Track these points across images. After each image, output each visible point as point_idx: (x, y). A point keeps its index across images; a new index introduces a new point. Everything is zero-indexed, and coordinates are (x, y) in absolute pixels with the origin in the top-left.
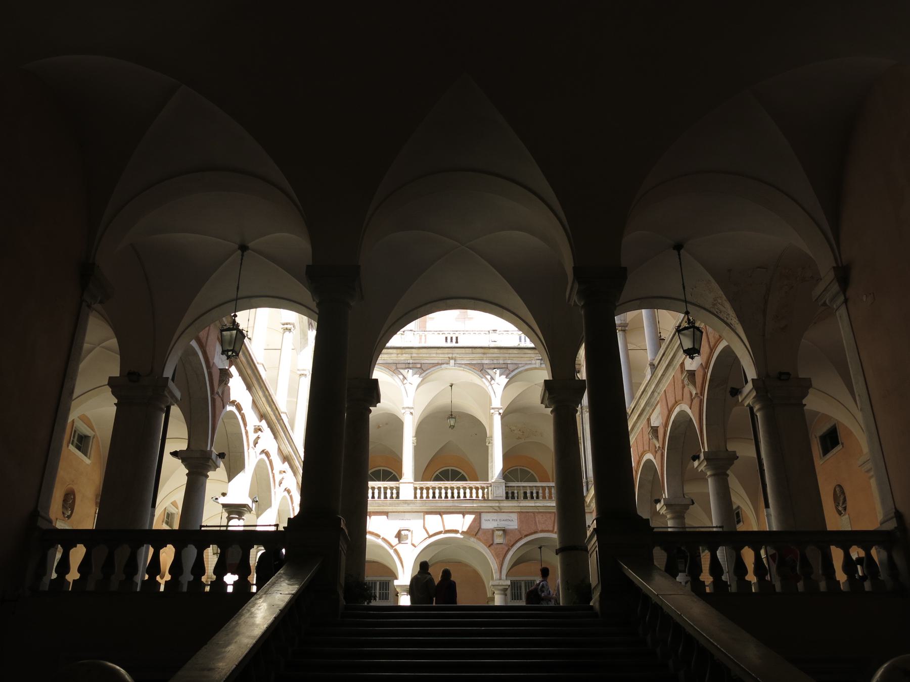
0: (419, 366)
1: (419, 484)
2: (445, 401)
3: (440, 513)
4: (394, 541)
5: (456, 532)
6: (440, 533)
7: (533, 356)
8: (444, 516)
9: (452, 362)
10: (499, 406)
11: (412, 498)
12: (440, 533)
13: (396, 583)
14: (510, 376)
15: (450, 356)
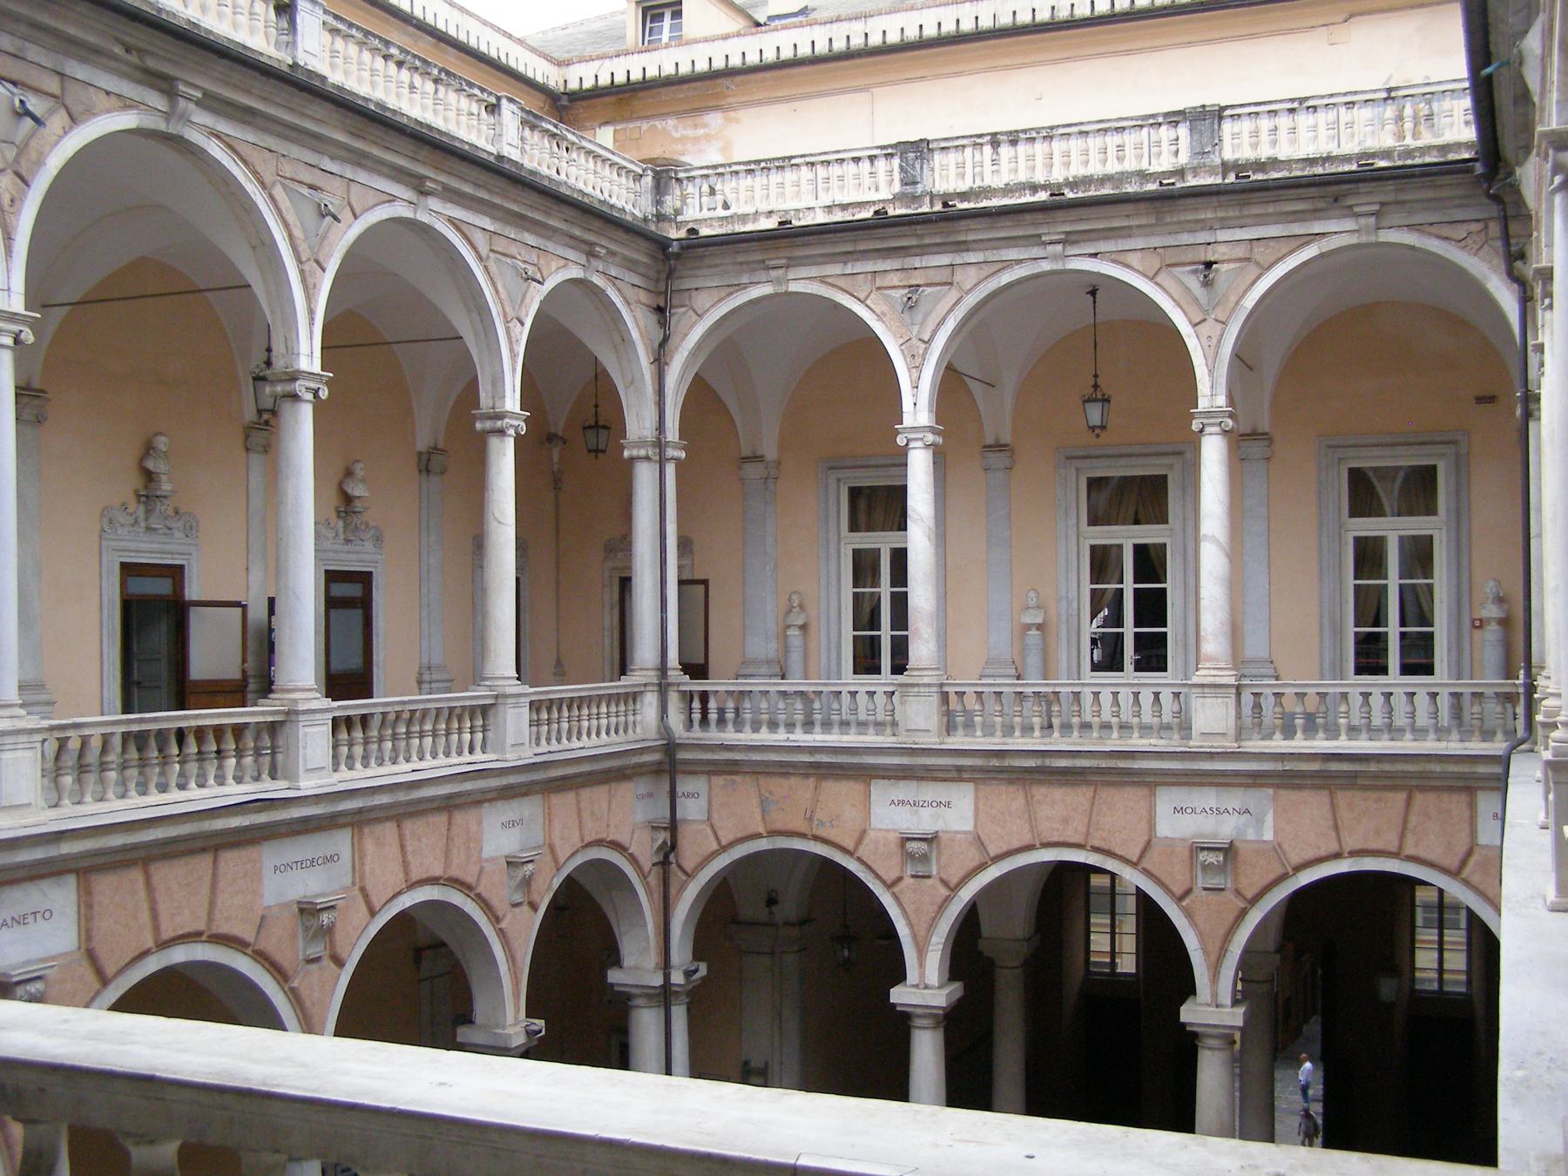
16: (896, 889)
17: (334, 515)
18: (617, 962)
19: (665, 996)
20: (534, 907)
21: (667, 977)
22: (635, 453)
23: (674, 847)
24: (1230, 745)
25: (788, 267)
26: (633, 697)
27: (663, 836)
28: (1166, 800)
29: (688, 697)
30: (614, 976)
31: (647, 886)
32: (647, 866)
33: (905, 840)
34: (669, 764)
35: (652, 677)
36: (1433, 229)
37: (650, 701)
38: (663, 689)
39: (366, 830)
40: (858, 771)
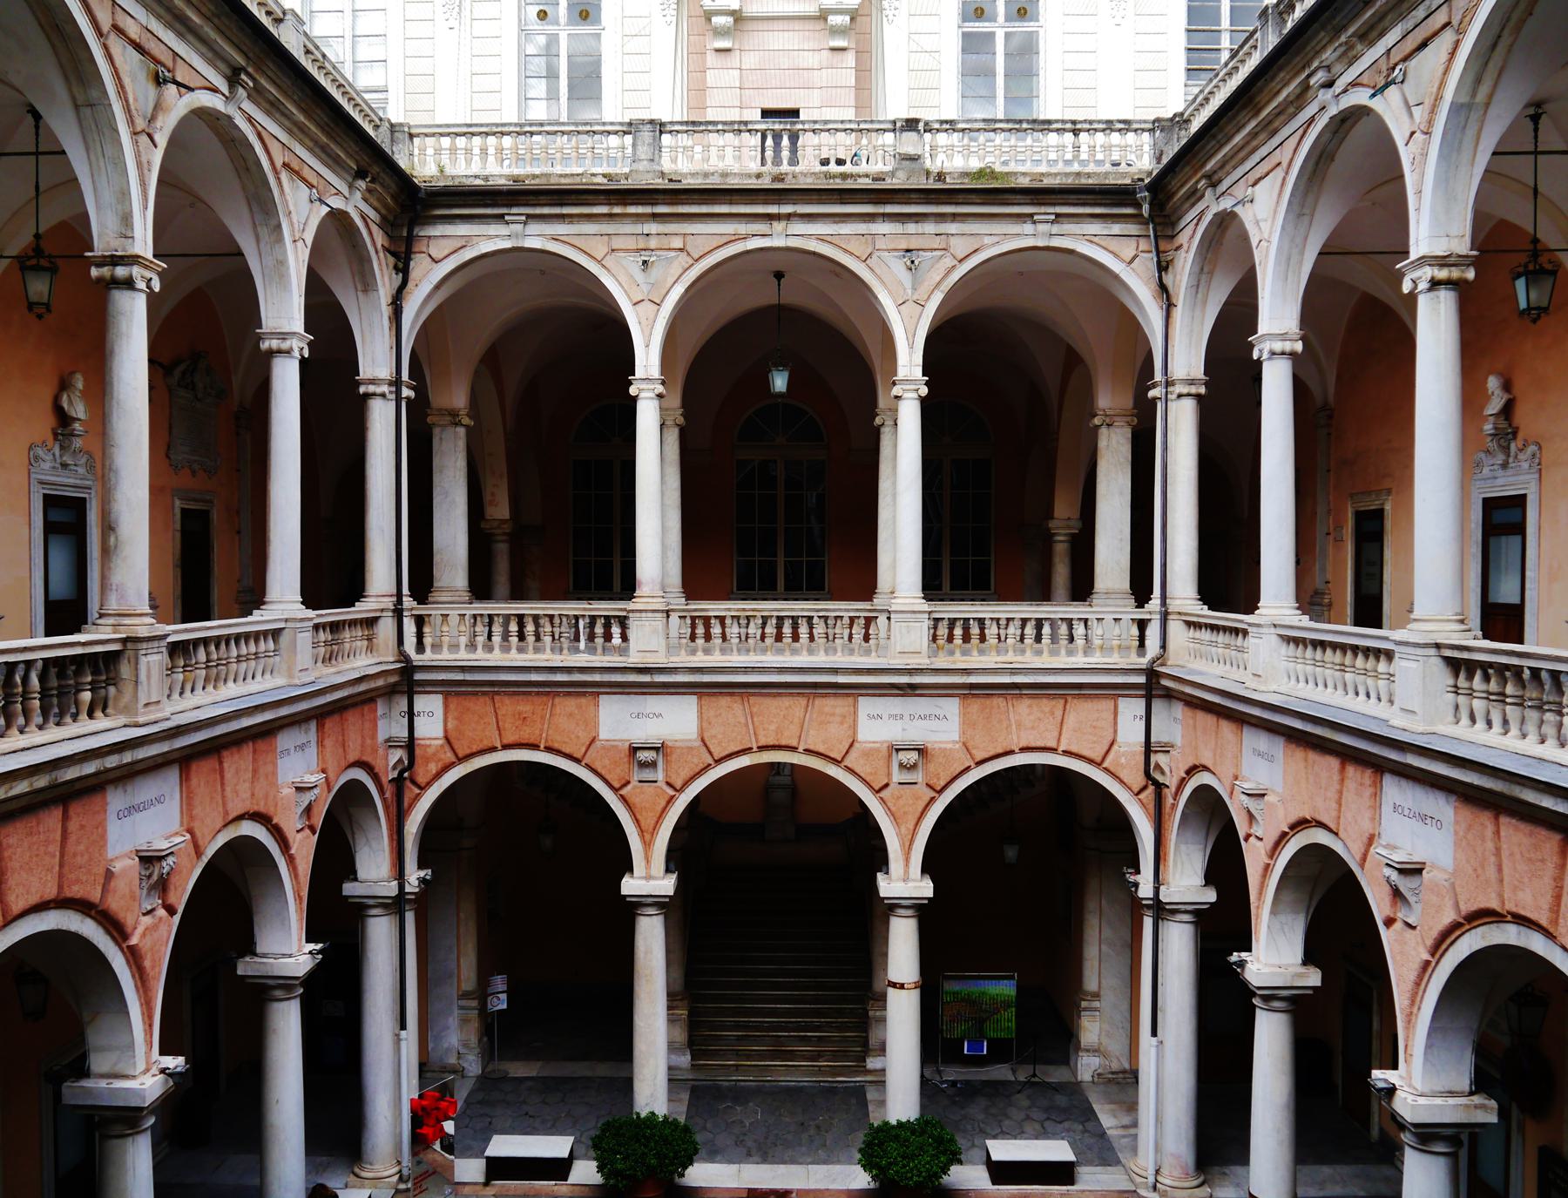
0: (677, 243)
9: (778, 226)
16: (623, 792)
17: (51, 437)
19: (396, 906)
20: (312, 829)
21: (401, 887)
22: (371, 389)
24: (923, 661)
25: (525, 223)
26: (370, 623)
27: (396, 755)
28: (867, 705)
29: (420, 621)
30: (349, 889)
31: (384, 800)
32: (384, 780)
33: (634, 750)
34: (406, 682)
35: (389, 603)
36: (1096, 239)
37: (386, 627)
38: (398, 613)
39: (194, 767)
40: (587, 688)
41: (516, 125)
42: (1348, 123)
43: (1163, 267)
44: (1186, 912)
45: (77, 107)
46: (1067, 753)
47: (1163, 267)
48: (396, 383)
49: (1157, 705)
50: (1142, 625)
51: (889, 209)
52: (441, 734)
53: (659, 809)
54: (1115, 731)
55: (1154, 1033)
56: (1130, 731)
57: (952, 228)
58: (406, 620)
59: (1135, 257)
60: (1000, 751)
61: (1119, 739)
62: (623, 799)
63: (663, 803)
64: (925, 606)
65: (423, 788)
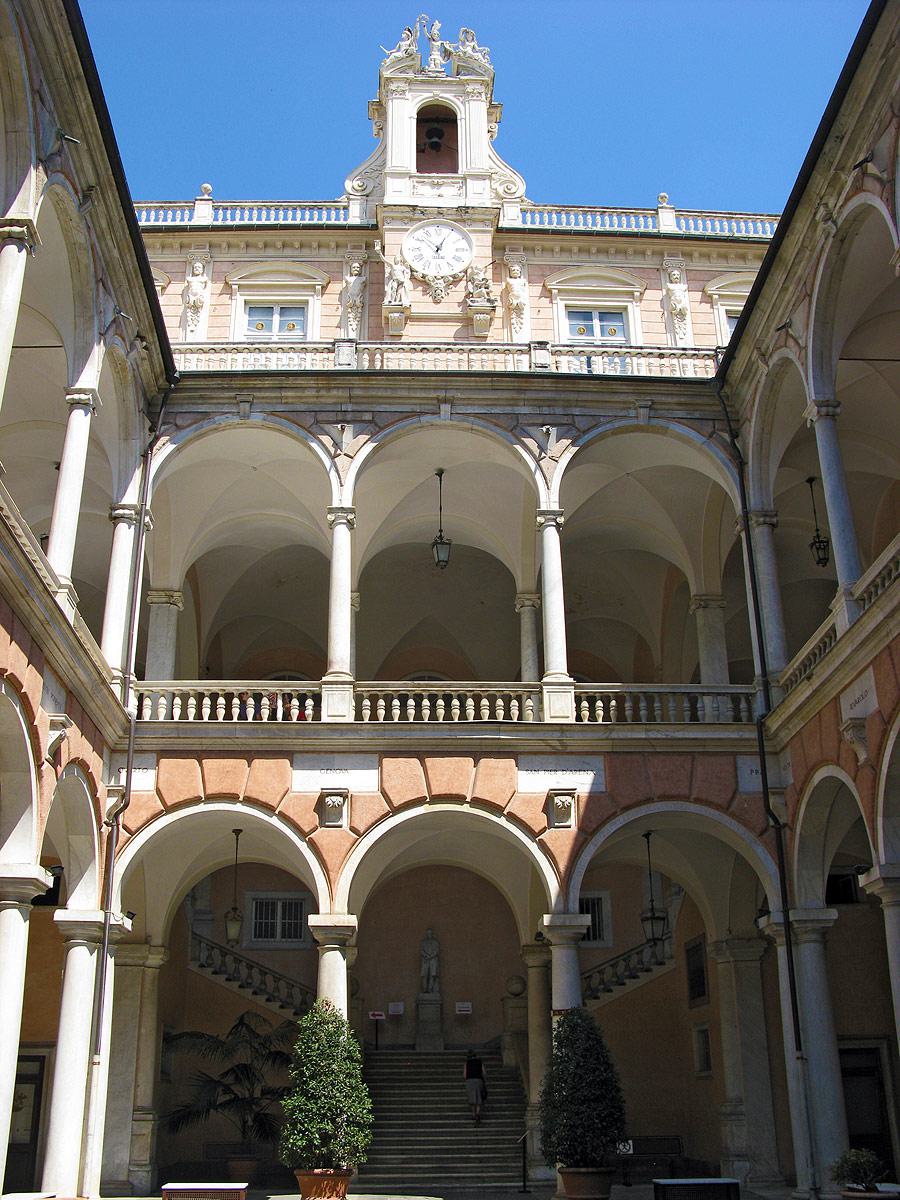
0: (368, 417)
1: (369, 686)
2: (423, 520)
3: (421, 755)
4: (308, 819)
5: (459, 799)
6: (420, 801)
7: (631, 398)
8: (429, 761)
9: (445, 408)
10: (555, 507)
11: (350, 718)
12: (420, 801)
13: (313, 920)
14: (581, 442)
15: (442, 394)
18: (64, 906)
19: (98, 937)
23: (126, 806)
29: (141, 698)
38: (125, 684)
41: (248, 343)
42: (845, 245)
43: (735, 435)
44: (814, 931)
45: (6, 132)
46: (698, 801)
47: (735, 435)
48: (140, 512)
49: (769, 760)
50: (749, 697)
51: (528, 395)
52: (152, 787)
53: (345, 849)
54: (737, 782)
55: (799, 1047)
56: (750, 782)
57: (576, 411)
58: (132, 693)
59: (714, 432)
60: (641, 798)
61: (741, 790)
62: (312, 845)
63: (348, 845)
64: (571, 680)
65: (132, 833)
